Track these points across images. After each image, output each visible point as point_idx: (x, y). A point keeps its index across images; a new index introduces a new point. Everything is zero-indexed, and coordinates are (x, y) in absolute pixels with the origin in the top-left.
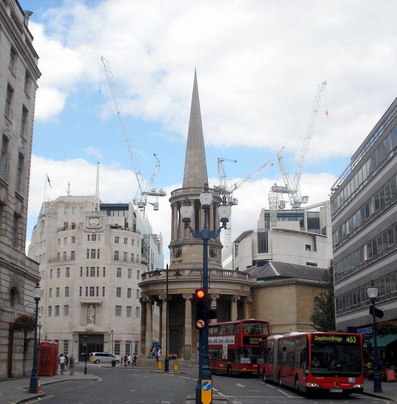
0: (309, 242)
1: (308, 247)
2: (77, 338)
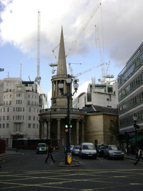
0: (108, 97)
1: (108, 100)
2: (12, 137)
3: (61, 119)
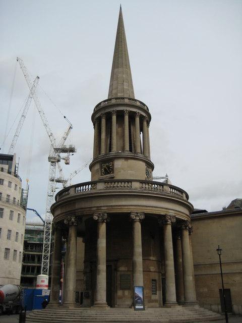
3: (146, 214)
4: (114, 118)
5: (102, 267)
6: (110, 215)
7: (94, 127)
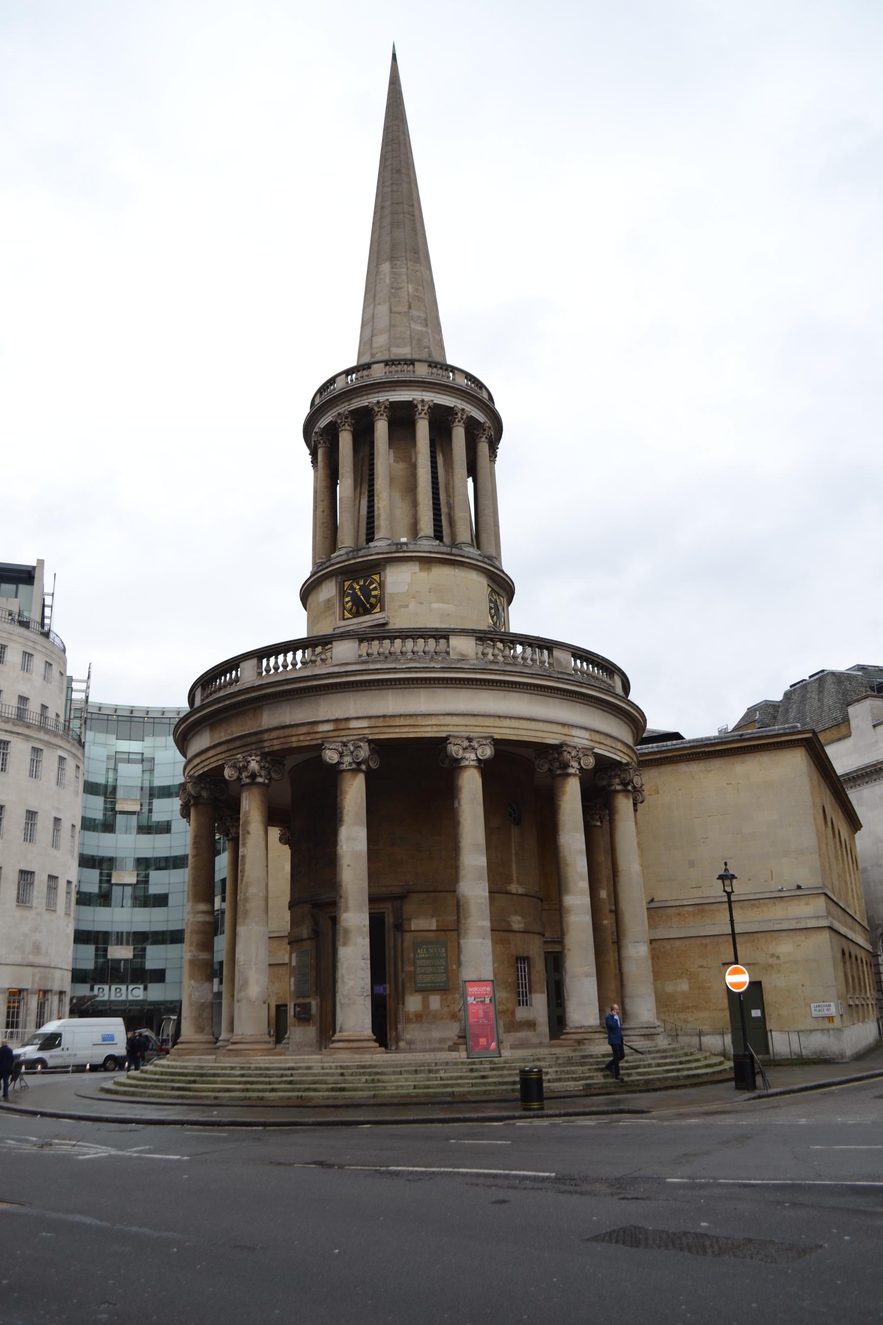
3: (497, 743)
4: (381, 427)
5: (355, 918)
6: (379, 747)
7: (314, 462)
